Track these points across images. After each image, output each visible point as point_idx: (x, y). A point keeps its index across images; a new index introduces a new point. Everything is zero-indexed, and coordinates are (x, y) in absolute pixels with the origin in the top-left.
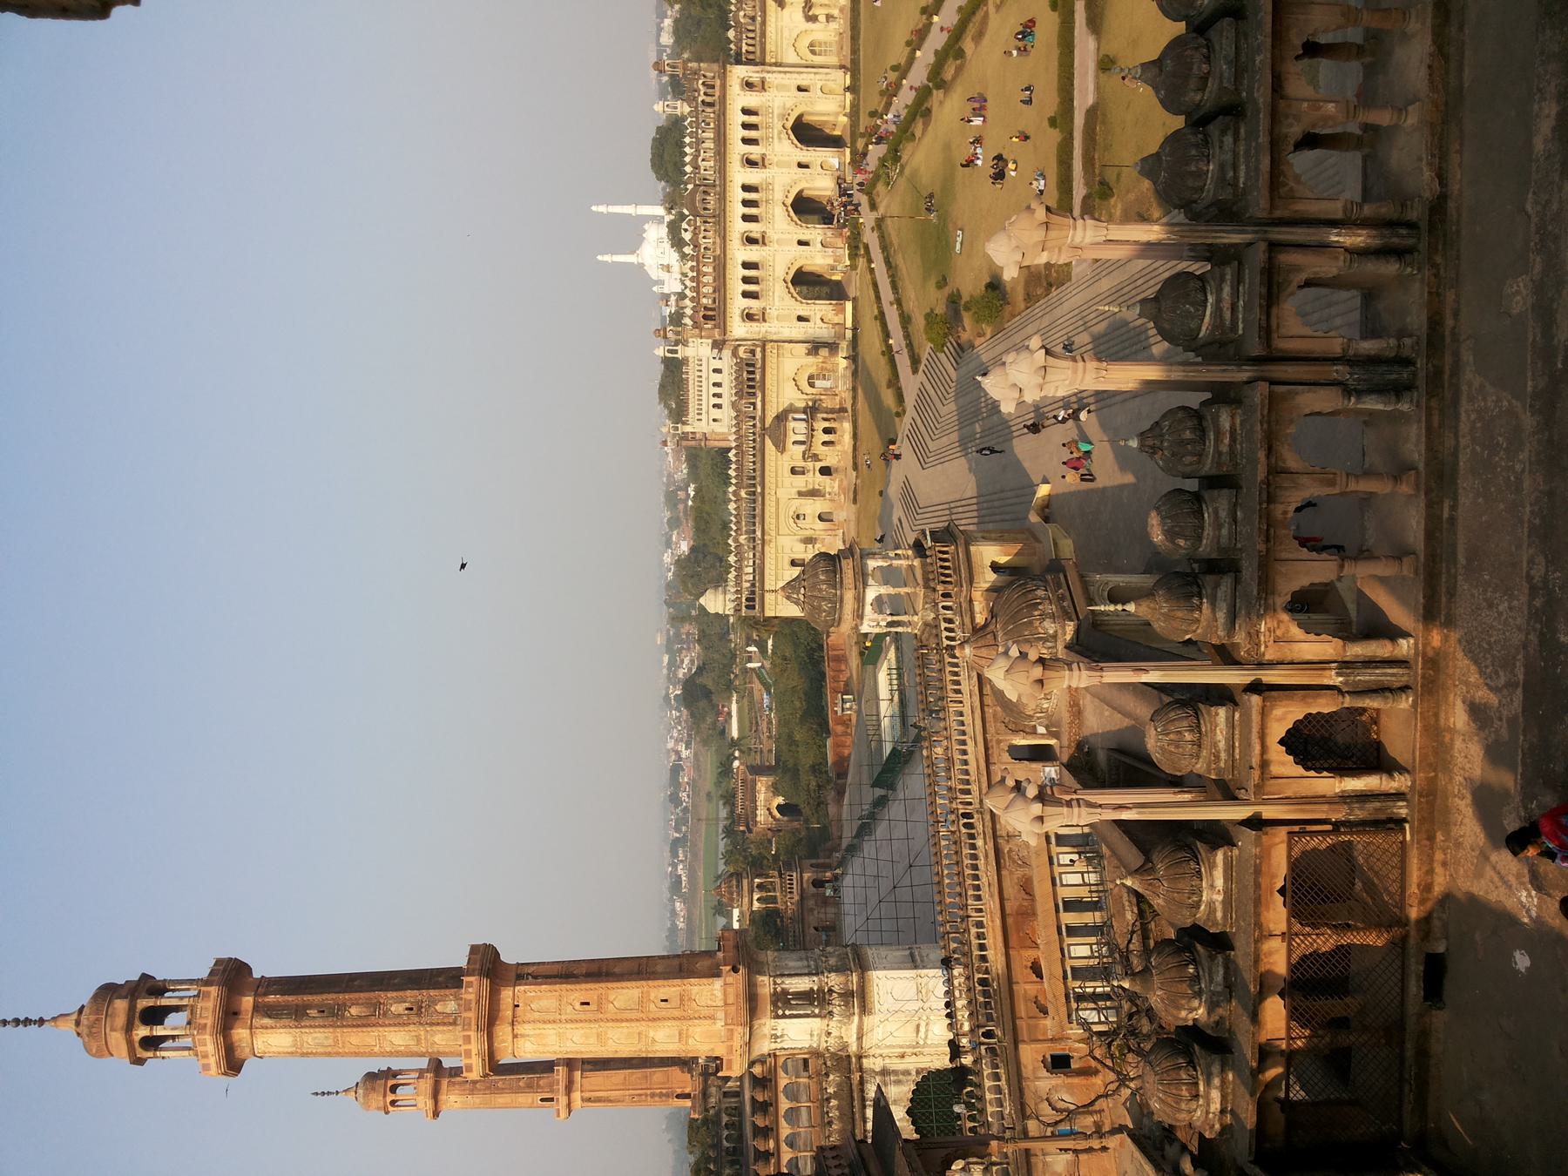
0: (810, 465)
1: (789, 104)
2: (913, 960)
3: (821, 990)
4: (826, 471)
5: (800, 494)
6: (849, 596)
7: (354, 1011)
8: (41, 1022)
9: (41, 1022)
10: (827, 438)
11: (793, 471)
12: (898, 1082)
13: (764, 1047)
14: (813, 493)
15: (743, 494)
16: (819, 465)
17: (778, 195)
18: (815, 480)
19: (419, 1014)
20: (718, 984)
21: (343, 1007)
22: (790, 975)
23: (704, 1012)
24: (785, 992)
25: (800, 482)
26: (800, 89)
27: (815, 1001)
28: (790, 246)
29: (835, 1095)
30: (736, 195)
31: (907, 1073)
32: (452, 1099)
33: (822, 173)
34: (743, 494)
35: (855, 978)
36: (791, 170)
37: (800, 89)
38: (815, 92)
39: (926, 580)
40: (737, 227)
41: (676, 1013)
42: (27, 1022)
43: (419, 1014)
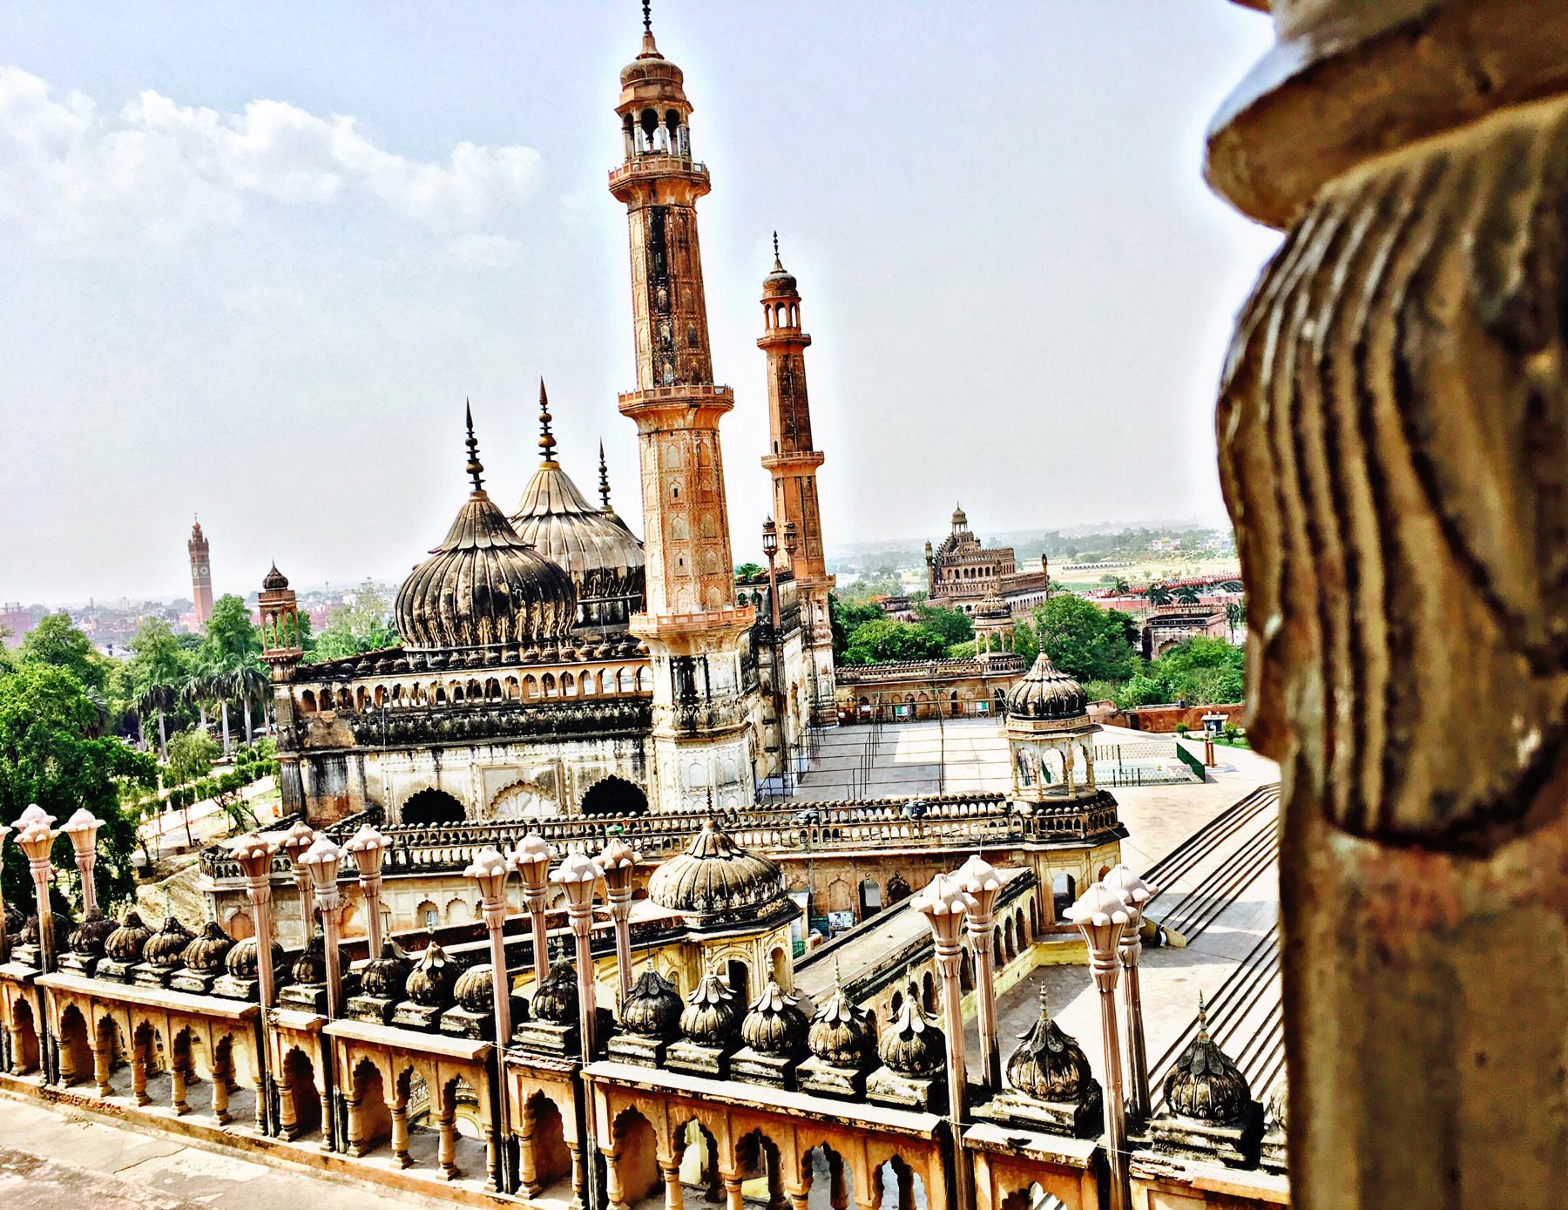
2: (726, 784)
3: (697, 700)
6: (1028, 726)
7: (662, 293)
8: (647, 23)
9: (647, 23)
12: (635, 769)
13: (653, 654)
19: (662, 349)
20: (696, 609)
21: (666, 283)
22: (707, 672)
23: (673, 598)
24: (693, 668)
27: (688, 696)
29: (622, 713)
31: (643, 776)
35: (706, 730)
39: (1044, 805)
41: (671, 573)
43: (662, 349)
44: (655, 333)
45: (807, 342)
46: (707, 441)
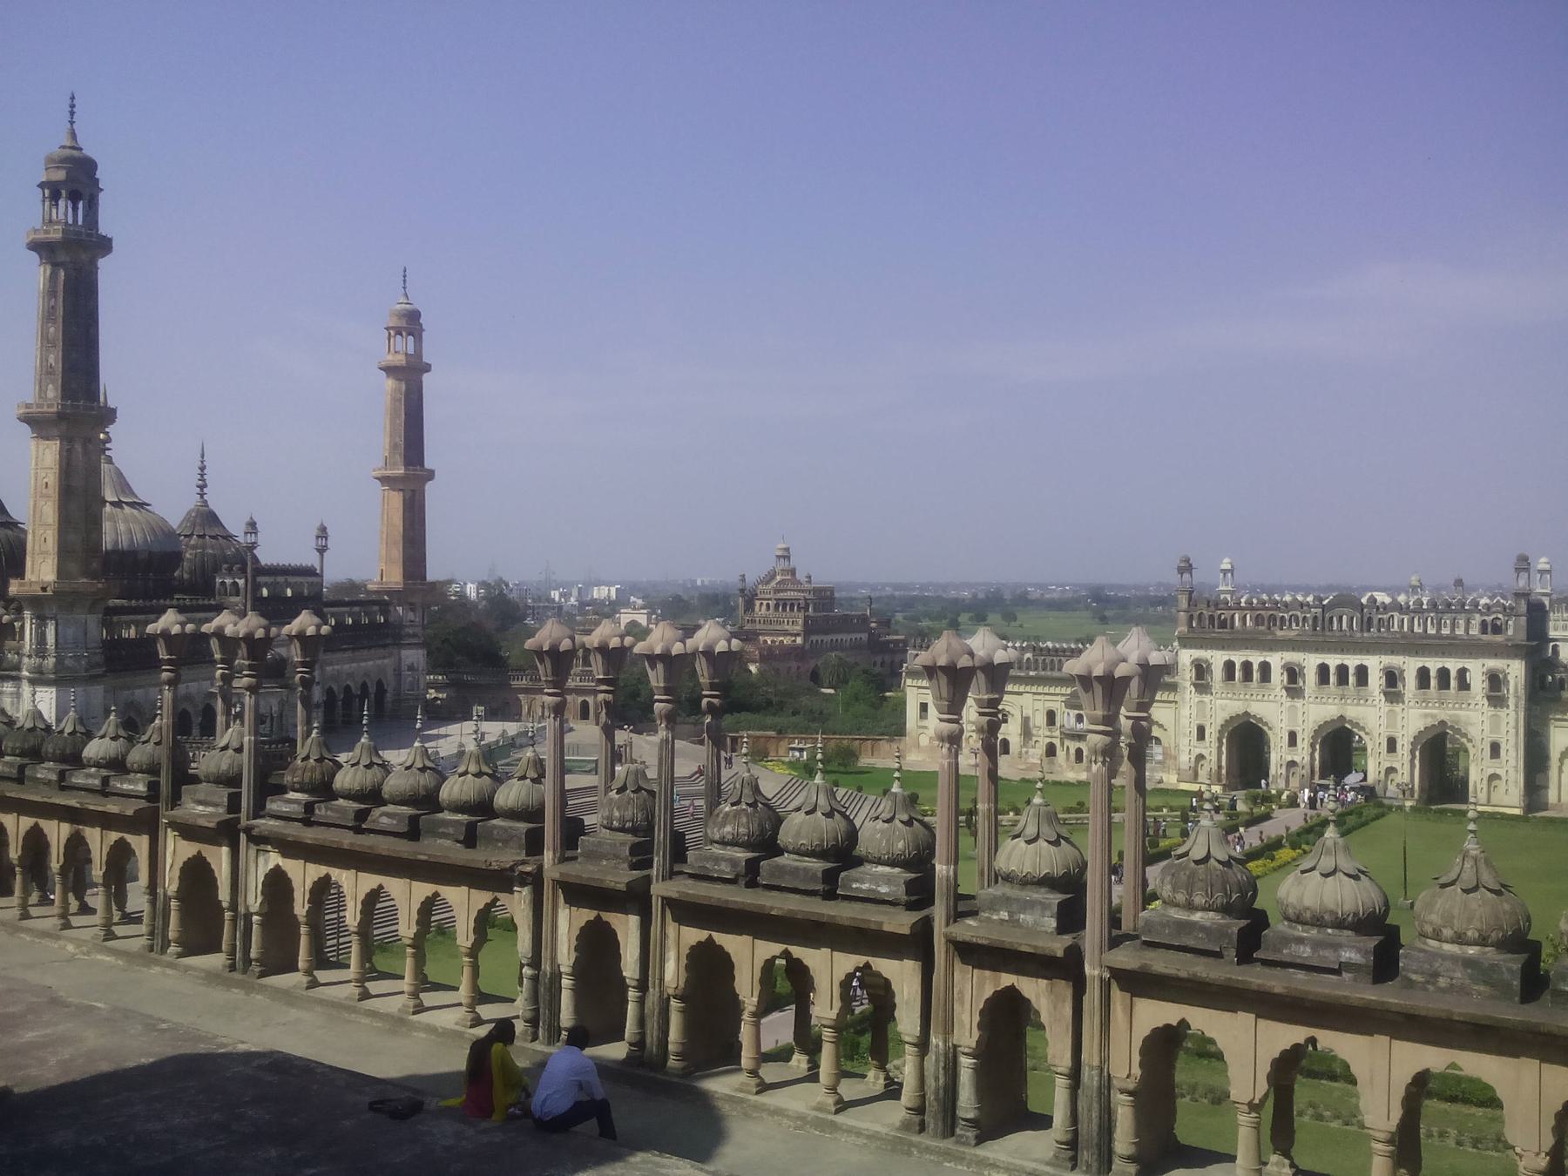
0: (1057, 733)
1: (1473, 732)
4: (1051, 751)
5: (1026, 721)
7: (52, 330)
8: (72, 123)
9: (72, 123)
10: (1072, 751)
11: (1051, 717)
14: (1027, 732)
15: (1028, 655)
16: (1057, 742)
17: (1352, 712)
18: (1043, 736)
21: (54, 321)
25: (1040, 720)
26: (1495, 749)
28: (1292, 722)
30: (1352, 661)
32: (389, 384)
33: (1290, 757)
34: (1028, 655)
36: (1390, 728)
37: (1495, 749)
38: (1491, 767)
40: (1310, 662)
42: (72, 113)
44: (44, 359)
45: (427, 368)
46: (78, 448)
